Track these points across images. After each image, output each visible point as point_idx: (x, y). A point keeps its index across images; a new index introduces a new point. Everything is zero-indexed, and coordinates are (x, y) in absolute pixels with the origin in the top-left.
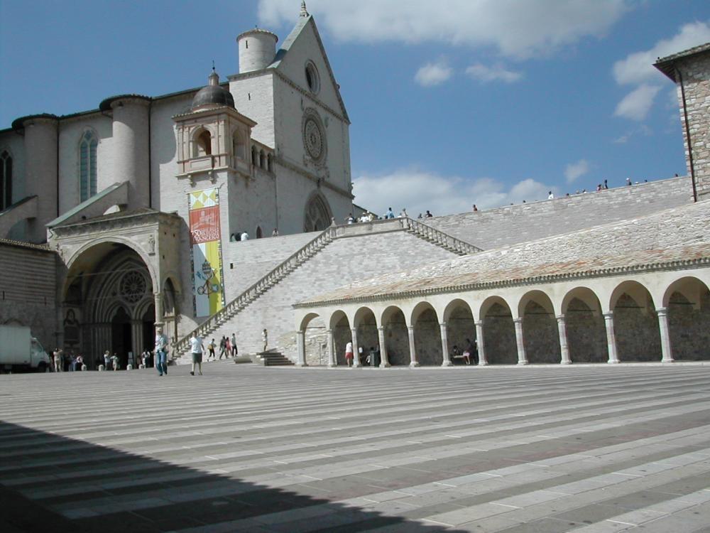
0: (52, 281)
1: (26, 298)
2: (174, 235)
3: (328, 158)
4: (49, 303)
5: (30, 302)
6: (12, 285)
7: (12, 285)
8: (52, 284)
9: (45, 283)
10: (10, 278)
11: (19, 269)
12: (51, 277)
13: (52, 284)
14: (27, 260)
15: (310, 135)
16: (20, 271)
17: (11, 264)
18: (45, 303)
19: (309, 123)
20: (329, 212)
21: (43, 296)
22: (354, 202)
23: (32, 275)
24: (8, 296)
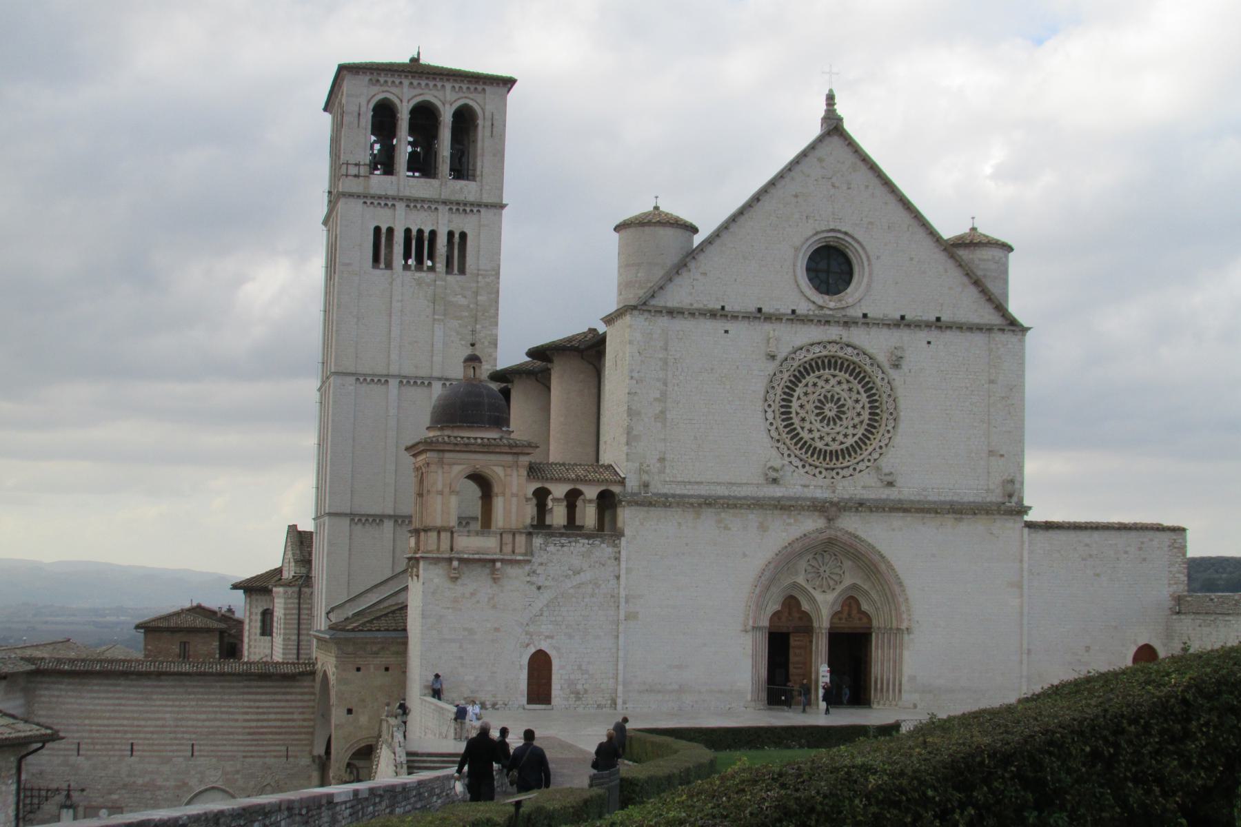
0: (304, 720)
1: (244, 751)
2: (387, 669)
3: (897, 440)
4: (296, 757)
5: (252, 757)
6: (214, 733)
7: (214, 733)
8: (305, 724)
9: (285, 724)
10: (207, 723)
11: (230, 707)
12: (300, 713)
13: (305, 724)
14: (246, 690)
15: (810, 407)
16: (231, 710)
17: (209, 700)
18: (287, 757)
19: (811, 379)
20: (883, 567)
21: (284, 745)
22: (1026, 518)
23: (257, 713)
24: (200, 751)
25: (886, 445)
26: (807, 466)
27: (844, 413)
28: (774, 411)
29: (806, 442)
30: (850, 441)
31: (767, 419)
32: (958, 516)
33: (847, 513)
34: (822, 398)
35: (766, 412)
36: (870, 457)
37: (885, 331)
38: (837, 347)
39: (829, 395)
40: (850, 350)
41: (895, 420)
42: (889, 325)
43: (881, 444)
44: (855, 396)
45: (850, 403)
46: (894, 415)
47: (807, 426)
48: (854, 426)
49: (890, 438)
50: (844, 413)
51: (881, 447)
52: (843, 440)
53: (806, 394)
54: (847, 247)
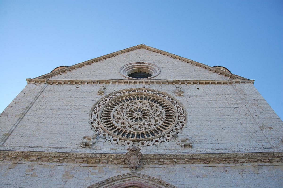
25: (181, 128)
26: (118, 140)
27: (148, 115)
28: (97, 115)
29: (118, 129)
30: (152, 127)
31: (91, 118)
32: (257, 164)
33: (151, 165)
34: (132, 110)
35: (92, 115)
36: (169, 134)
37: (170, 85)
38: (141, 91)
39: (137, 109)
40: (150, 92)
41: (185, 117)
42: (172, 83)
43: (178, 127)
44: (155, 108)
45: (151, 111)
46: (184, 114)
47: (121, 121)
48: (156, 121)
49: (183, 125)
50: (148, 115)
51: (176, 129)
52: (147, 127)
53: (122, 108)
54: (148, 68)
